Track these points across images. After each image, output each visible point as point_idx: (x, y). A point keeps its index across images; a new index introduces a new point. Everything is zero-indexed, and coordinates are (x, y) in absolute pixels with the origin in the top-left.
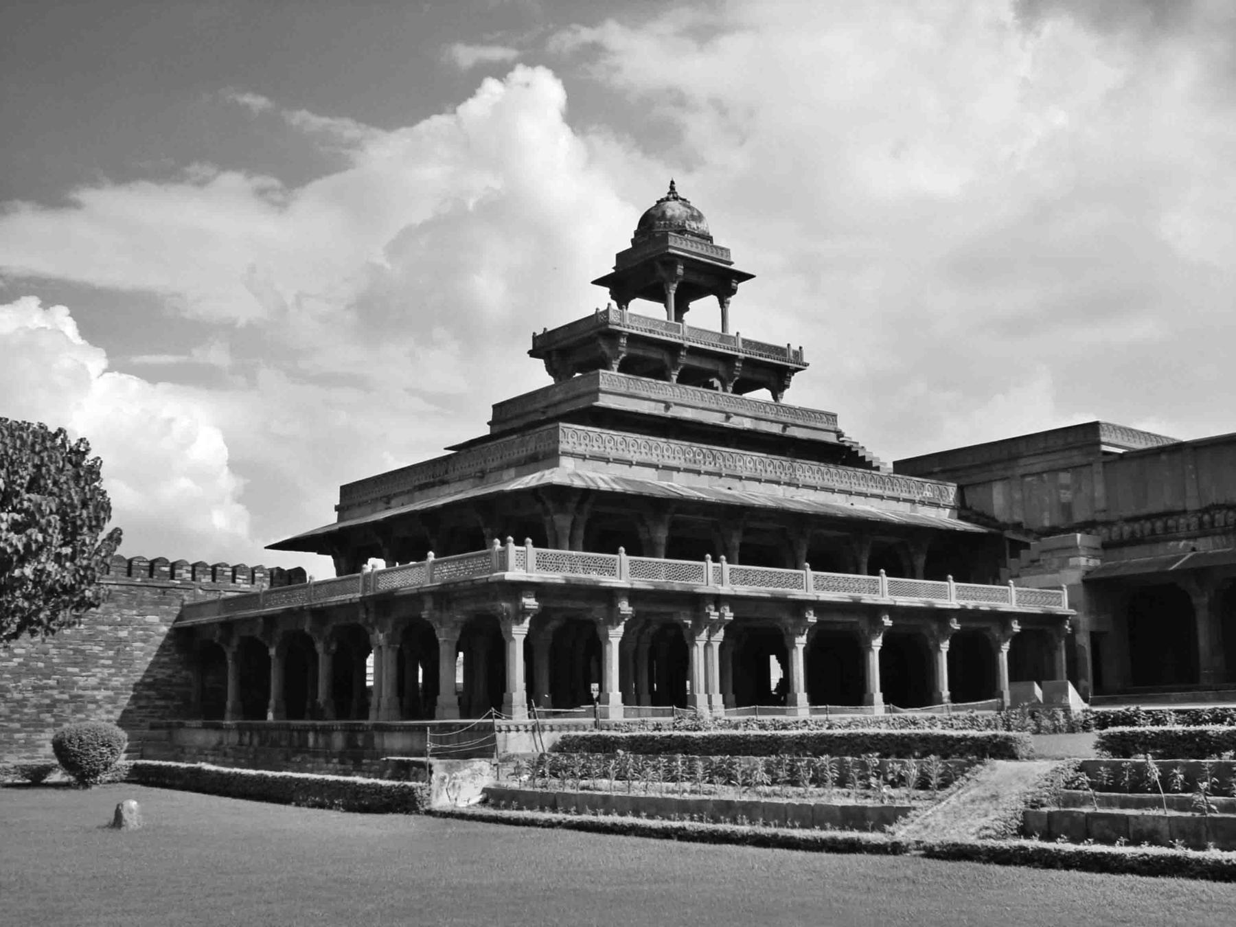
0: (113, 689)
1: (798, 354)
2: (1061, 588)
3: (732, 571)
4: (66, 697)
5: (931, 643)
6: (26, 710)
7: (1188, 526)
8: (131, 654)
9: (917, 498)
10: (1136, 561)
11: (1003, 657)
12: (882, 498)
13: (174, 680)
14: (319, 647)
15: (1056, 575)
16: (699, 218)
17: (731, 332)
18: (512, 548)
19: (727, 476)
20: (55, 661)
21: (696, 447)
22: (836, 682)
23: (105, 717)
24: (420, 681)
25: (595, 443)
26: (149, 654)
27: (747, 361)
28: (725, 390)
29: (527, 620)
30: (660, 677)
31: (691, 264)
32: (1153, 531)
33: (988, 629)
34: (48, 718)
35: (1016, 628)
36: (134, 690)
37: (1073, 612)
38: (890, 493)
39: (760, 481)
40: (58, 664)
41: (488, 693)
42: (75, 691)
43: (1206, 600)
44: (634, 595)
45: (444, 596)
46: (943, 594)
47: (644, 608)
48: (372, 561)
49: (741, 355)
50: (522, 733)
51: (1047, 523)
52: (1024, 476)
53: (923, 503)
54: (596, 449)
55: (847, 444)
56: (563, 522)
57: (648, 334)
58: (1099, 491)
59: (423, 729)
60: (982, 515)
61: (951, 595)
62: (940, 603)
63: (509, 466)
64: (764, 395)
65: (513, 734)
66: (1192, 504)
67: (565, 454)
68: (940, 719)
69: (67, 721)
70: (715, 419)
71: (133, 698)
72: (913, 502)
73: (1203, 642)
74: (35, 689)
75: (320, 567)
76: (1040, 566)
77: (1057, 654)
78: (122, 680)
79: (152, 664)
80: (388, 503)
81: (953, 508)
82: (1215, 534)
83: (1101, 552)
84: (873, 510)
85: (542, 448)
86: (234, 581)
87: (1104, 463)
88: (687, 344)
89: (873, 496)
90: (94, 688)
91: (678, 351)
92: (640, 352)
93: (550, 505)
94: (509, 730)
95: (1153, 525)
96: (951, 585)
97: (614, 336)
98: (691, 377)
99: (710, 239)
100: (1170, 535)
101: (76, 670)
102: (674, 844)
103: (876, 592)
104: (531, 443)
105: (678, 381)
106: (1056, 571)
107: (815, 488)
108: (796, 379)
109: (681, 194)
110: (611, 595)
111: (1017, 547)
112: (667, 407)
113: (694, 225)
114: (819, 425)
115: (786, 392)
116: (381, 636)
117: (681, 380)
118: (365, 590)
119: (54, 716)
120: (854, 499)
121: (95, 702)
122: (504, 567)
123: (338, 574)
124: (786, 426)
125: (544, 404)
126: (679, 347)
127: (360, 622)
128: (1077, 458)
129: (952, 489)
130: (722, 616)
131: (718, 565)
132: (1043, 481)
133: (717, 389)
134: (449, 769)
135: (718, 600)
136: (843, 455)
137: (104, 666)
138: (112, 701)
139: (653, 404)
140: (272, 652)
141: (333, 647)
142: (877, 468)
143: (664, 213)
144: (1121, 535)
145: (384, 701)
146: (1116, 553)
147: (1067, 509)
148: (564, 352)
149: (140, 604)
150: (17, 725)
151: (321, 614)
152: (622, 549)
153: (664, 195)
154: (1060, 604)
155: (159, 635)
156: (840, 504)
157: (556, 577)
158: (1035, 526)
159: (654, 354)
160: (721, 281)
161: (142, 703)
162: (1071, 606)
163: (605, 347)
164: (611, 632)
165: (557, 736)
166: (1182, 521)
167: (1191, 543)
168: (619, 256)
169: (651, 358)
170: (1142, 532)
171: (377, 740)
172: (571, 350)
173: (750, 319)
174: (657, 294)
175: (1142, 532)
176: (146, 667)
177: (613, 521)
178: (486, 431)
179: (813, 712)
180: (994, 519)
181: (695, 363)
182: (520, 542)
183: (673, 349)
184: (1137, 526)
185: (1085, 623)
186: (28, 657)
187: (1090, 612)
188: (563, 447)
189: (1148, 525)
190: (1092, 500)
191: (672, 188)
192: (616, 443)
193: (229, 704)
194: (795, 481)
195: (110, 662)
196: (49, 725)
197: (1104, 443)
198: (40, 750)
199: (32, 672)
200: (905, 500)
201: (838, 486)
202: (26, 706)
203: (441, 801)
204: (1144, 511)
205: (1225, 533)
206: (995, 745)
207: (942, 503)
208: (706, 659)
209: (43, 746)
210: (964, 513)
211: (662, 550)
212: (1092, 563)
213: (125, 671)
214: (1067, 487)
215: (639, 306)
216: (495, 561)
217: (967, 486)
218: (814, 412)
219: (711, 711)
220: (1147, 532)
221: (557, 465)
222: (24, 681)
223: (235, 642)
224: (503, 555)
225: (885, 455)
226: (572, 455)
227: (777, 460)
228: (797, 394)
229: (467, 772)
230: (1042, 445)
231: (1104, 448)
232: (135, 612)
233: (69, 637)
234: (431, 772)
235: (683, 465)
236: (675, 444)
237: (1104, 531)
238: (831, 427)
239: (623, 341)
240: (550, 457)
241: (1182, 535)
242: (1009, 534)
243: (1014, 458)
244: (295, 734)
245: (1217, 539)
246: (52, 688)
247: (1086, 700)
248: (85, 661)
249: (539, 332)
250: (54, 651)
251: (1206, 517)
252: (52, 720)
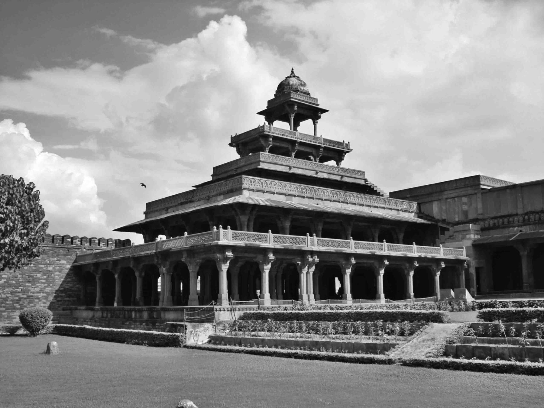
0: (46, 293)
1: (348, 145)
2: (463, 248)
3: (318, 240)
4: (25, 296)
5: (406, 272)
6: (7, 302)
7: (518, 221)
8: (54, 277)
9: (400, 208)
10: (496, 236)
11: (437, 278)
12: (384, 208)
13: (73, 289)
14: (137, 274)
15: (461, 243)
16: (304, 85)
17: (318, 135)
18: (222, 230)
19: (316, 198)
20: (21, 280)
21: (303, 186)
22: (364, 289)
23: (42, 305)
24: (181, 289)
25: (258, 184)
26: (62, 278)
27: (325, 148)
28: (315, 161)
29: (228, 262)
30: (287, 287)
31: (300, 105)
32: (503, 223)
33: (431, 266)
34: (18, 306)
35: (443, 265)
36: (55, 293)
37: (468, 258)
39: (331, 201)
40: (22, 282)
41: (211, 294)
42: (30, 294)
43: (526, 253)
44: (275, 251)
45: (192, 251)
46: (411, 251)
47: (279, 257)
48: (160, 236)
49: (323, 146)
50: (226, 312)
51: (457, 220)
52: (446, 199)
53: (402, 211)
54: (259, 187)
55: (369, 185)
56: (244, 219)
57: (282, 136)
58: (480, 205)
59: (183, 309)
60: (428, 216)
61: (415, 251)
62: (410, 255)
63: (220, 194)
64: (332, 163)
65: (222, 312)
66: (520, 211)
67: (245, 189)
68: (410, 305)
69: (26, 307)
70: (311, 174)
71: (55, 297)
72: (398, 210)
73: (525, 271)
74: (12, 293)
75: (137, 239)
76: (454, 239)
77: (461, 276)
78: (50, 289)
79: (63, 282)
80: (167, 210)
81: (415, 213)
82: (530, 224)
83: (480, 232)
84: (381, 214)
85: (236, 186)
86: (99, 245)
87: (482, 193)
88: (299, 140)
89: (380, 207)
90: (38, 292)
91: (295, 144)
92: (278, 144)
93: (239, 212)
94: (220, 310)
95: (503, 220)
96: (415, 246)
97: (266, 137)
98: (300, 155)
99: (309, 94)
100: (510, 225)
101: (30, 284)
102: (293, 360)
103: (382, 249)
104: (230, 184)
105: (295, 157)
106: (461, 241)
107: (355, 204)
108: (347, 156)
109: (296, 75)
110: (265, 251)
111: (444, 230)
112: (290, 168)
113: (302, 88)
114: (357, 176)
115: (343, 162)
116: (164, 269)
117: (296, 157)
118: (156, 250)
119: (20, 305)
120: (372, 209)
121: (38, 298)
122: (218, 239)
123: (145, 242)
124: (342, 177)
125: (236, 167)
126: (295, 142)
127: (155, 263)
128: (470, 191)
129: (415, 204)
130: (314, 260)
131: (312, 238)
132: (455, 201)
133: (312, 160)
134: (194, 327)
135: (312, 253)
136: (367, 189)
137: (42, 283)
138: (46, 298)
139: (284, 167)
140: (116, 276)
141: (143, 274)
142: (382, 195)
143: (289, 82)
144: (489, 225)
145: (165, 297)
146: (487, 232)
147: (466, 213)
148: (245, 144)
149: (58, 256)
150: (4, 309)
151: (137, 260)
152: (270, 231)
153: (289, 75)
154: (462, 255)
155: (66, 269)
156: (366, 211)
157: (241, 243)
158: (452, 221)
159: (284, 145)
160: (314, 113)
161: (59, 299)
162: (467, 256)
163: (262, 142)
164: (265, 267)
165: (241, 313)
166: (516, 218)
167: (520, 228)
168: (269, 102)
169: (283, 147)
170: (498, 223)
171: (162, 315)
172: (248, 143)
173: (327, 130)
174: (285, 119)
175: (498, 223)
176: (60, 283)
177: (266, 218)
178: (210, 179)
179: (354, 302)
180: (434, 218)
181: (302, 149)
182: (225, 228)
183: (293, 143)
184: (496, 221)
185: (473, 264)
186: (8, 279)
187: (475, 259)
188: (244, 186)
189: (501, 220)
190: (476, 209)
191: (292, 72)
192: (267, 184)
193: (97, 299)
194: (346, 201)
195: (44, 281)
196: (18, 309)
197: (482, 185)
198: (14, 320)
199: (10, 285)
200: (394, 209)
201: (365, 203)
202: (7, 300)
203: (190, 342)
204: (499, 214)
205: (534, 224)
206: (434, 316)
207: (411, 211)
208: (307, 279)
209: (15, 318)
210: (420, 215)
211: (288, 231)
212: (476, 237)
213: (51, 285)
214: (465, 204)
215: (278, 124)
216: (214, 236)
217: (422, 203)
218: (354, 170)
219: (309, 302)
220: (500, 223)
221: (242, 194)
222: (7, 290)
223: (100, 272)
224: (218, 233)
225: (386, 189)
226: (248, 189)
227: (338, 191)
228: (347, 162)
229: (202, 329)
230: (455, 185)
231: (482, 187)
232: (55, 259)
233: (27, 270)
234: (186, 329)
235: (297, 194)
236: (293, 185)
237: (482, 223)
238: (362, 177)
239: (271, 139)
240: (238, 190)
241: (516, 224)
242: (440, 224)
243: (442, 191)
244: (127, 313)
245: (531, 226)
246: (19, 292)
247: (473, 297)
248: (34, 280)
249: (234, 135)
250: (20, 276)
251: (526, 217)
252: (19, 307)
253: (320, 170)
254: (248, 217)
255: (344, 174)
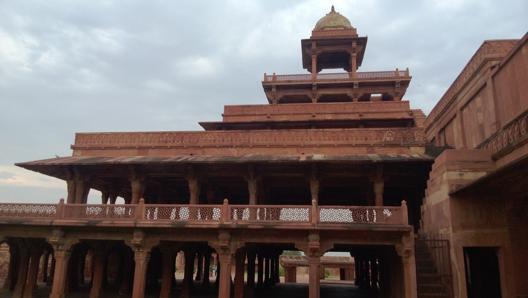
38: (341, 142)
39: (215, 147)
54: (96, 144)
58: (491, 106)
88: (315, 83)
107: (265, 146)
113: (331, 22)
114: (391, 110)
162: (410, 223)
239: (274, 90)
253: (319, 112)
254: (73, 182)
255: (365, 110)
